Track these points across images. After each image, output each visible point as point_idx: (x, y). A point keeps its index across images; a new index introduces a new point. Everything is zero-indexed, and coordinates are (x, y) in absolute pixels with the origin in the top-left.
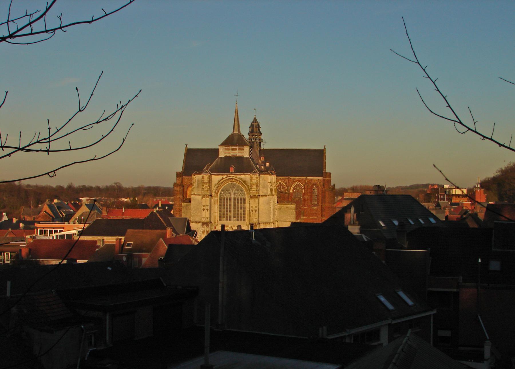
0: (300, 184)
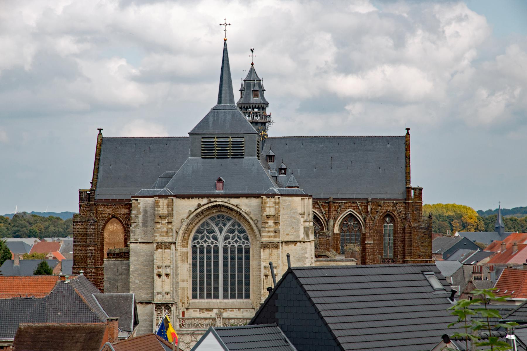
0: (356, 213)
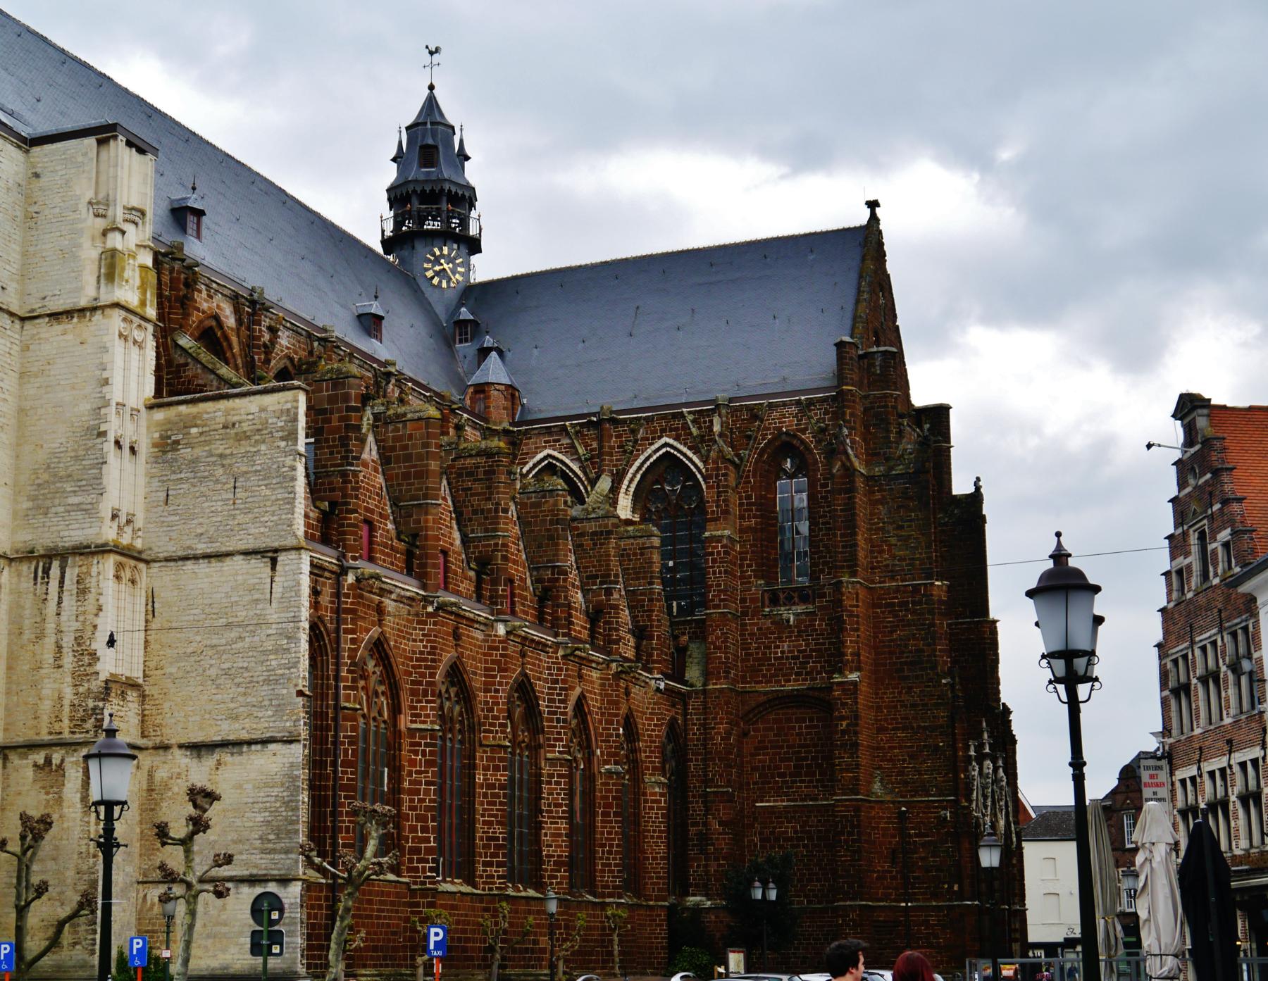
0: (685, 450)
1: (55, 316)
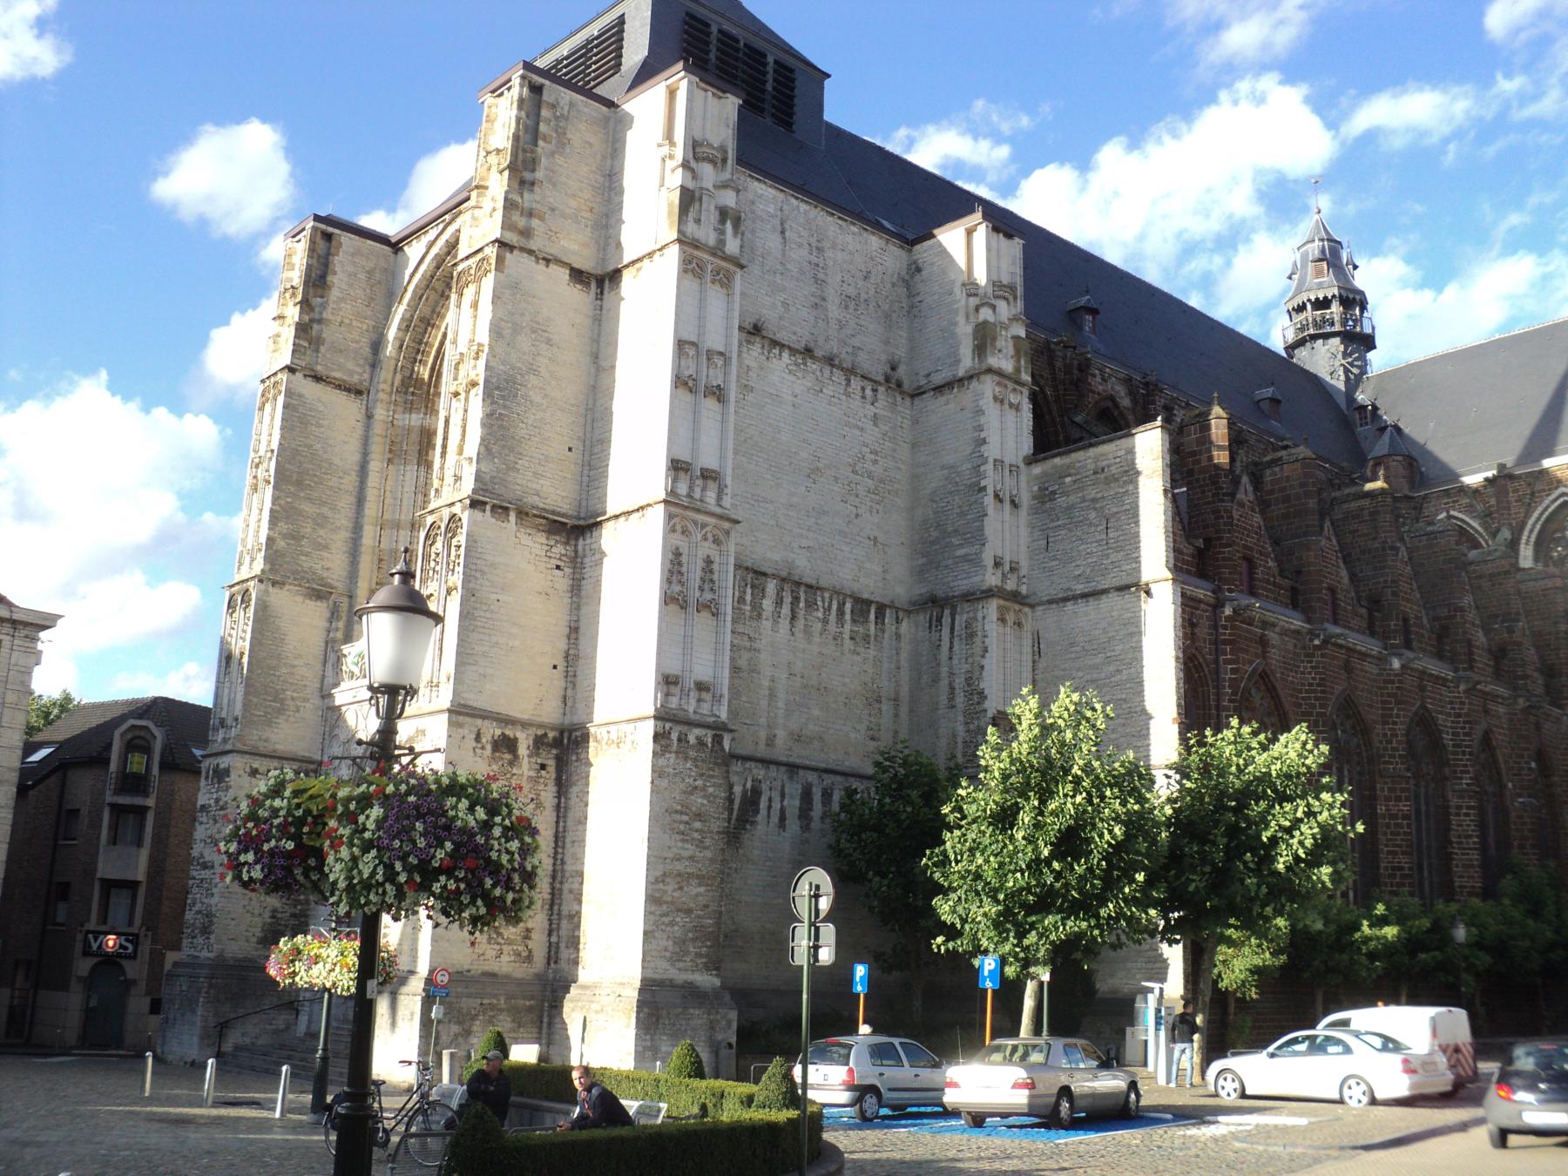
1: (939, 389)
